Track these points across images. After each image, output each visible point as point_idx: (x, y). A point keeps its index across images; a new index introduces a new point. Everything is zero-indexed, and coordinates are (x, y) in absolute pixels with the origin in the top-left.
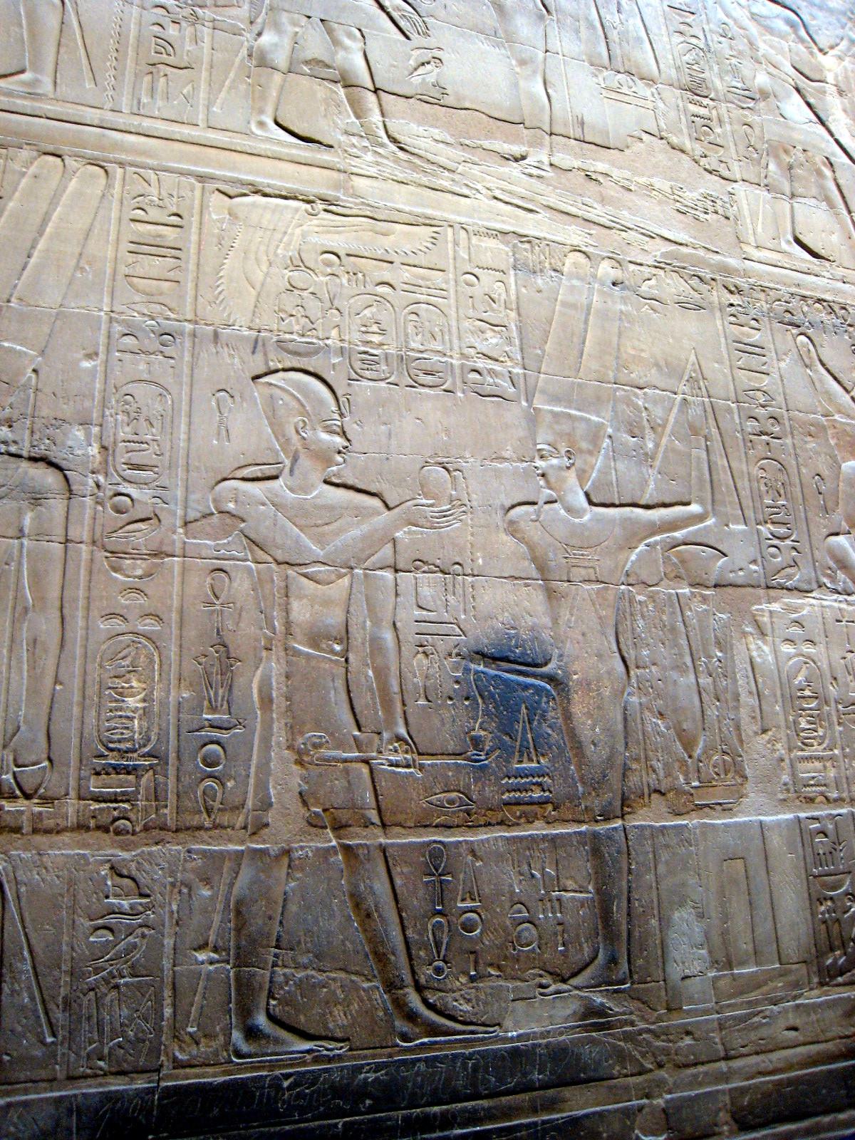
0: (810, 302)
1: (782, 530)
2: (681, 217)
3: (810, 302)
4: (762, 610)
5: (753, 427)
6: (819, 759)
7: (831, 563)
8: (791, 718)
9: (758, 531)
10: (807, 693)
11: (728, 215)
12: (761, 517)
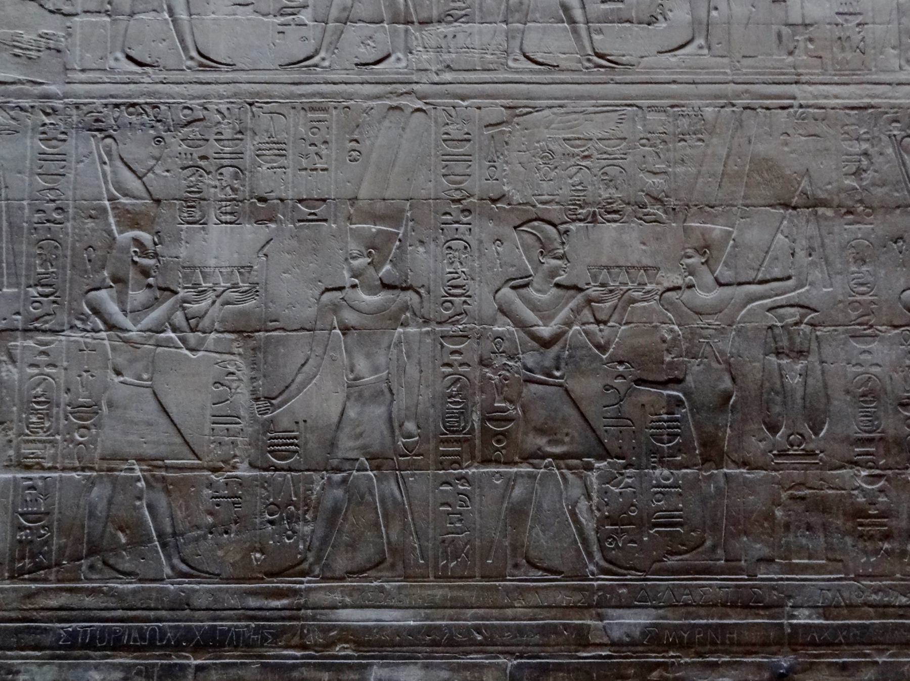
0: (123, 108)
1: (48, 290)
2: (17, 59)
3: (123, 108)
4: (17, 346)
5: (39, 218)
6: (40, 441)
7: (87, 310)
8: (24, 416)
9: (26, 293)
10: (42, 399)
11: (60, 47)
12: (32, 282)
